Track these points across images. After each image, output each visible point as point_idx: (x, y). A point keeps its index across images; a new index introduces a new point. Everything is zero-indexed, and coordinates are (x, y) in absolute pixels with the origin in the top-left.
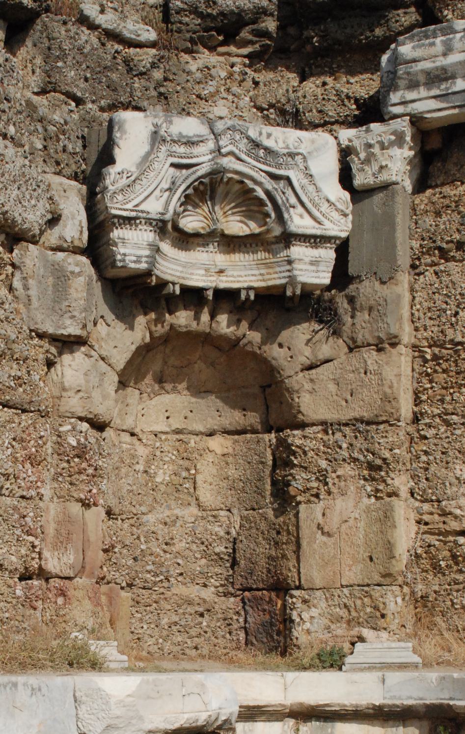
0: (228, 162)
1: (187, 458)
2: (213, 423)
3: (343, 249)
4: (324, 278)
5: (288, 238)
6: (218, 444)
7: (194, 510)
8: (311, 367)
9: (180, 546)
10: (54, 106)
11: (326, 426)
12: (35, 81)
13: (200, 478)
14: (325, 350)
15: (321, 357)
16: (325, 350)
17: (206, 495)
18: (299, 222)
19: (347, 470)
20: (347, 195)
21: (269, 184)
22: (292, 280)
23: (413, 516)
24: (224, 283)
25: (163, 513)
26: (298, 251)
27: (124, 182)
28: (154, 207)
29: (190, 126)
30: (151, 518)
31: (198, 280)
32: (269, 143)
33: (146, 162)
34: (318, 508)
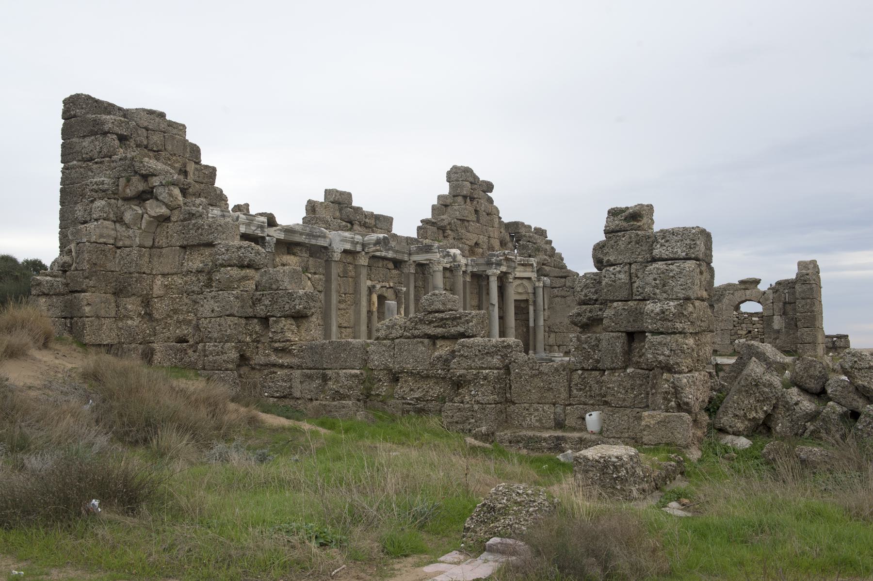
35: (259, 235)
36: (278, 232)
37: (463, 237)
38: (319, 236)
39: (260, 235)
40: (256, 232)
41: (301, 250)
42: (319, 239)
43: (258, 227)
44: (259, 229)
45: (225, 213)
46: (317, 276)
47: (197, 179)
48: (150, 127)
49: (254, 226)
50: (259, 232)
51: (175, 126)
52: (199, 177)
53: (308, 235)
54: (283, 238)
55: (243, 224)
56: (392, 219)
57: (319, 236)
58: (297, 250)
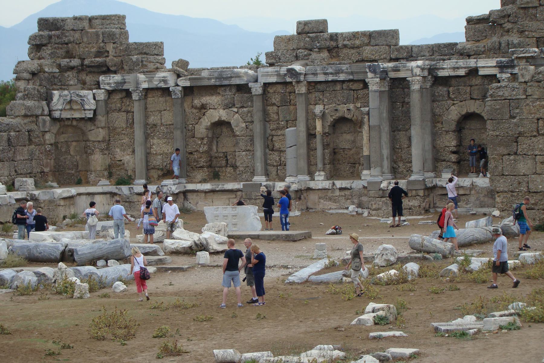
0: (73, 98)
1: (68, 147)
2: (73, 139)
3: (95, 111)
4: (92, 116)
5: (85, 110)
6: (74, 144)
7: (70, 156)
8: (90, 131)
9: (67, 163)
10: (41, 89)
11: (94, 142)
12: (38, 84)
13: (71, 150)
14: (93, 128)
15: (92, 129)
16: (93, 128)
17: (72, 153)
18: (87, 107)
19: (97, 150)
20: (95, 102)
21: (81, 101)
22: (86, 117)
23: (109, 158)
24: (73, 117)
25: (64, 157)
26: (86, 112)
27: (55, 104)
28: (60, 108)
29: (66, 92)
30: (62, 158)
31: (69, 117)
32: (80, 94)
33: (58, 100)
34: (93, 157)
35: (162, 87)
36: (183, 81)
37: (525, 28)
38: (231, 77)
39: (165, 86)
40: (160, 85)
41: (225, 90)
42: (233, 79)
43: (161, 82)
44: (162, 83)
45: (124, 77)
46: (245, 109)
47: (115, 55)
48: (75, 29)
49: (156, 81)
50: (163, 85)
51: (108, 18)
52: (116, 53)
53: (216, 78)
54: (189, 85)
55: (145, 81)
56: (398, 30)
57: (231, 77)
58: (220, 90)
